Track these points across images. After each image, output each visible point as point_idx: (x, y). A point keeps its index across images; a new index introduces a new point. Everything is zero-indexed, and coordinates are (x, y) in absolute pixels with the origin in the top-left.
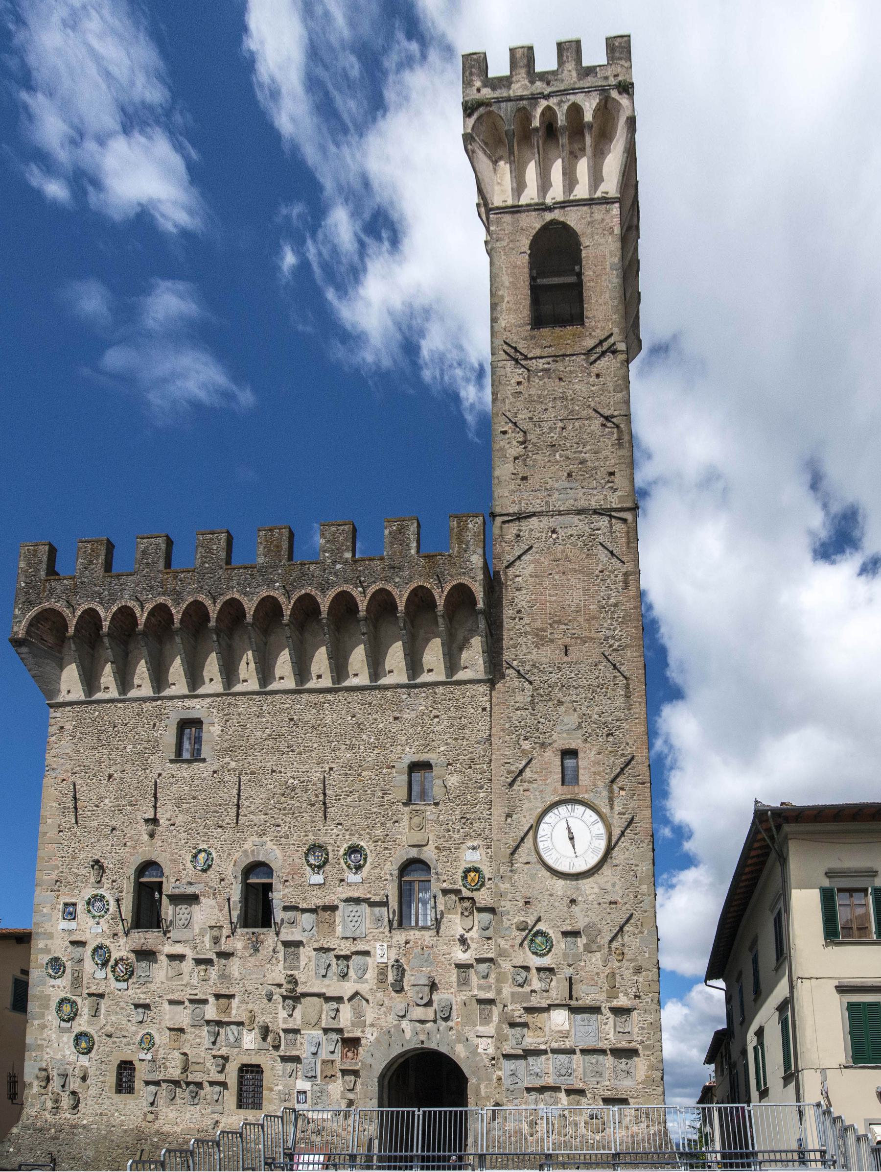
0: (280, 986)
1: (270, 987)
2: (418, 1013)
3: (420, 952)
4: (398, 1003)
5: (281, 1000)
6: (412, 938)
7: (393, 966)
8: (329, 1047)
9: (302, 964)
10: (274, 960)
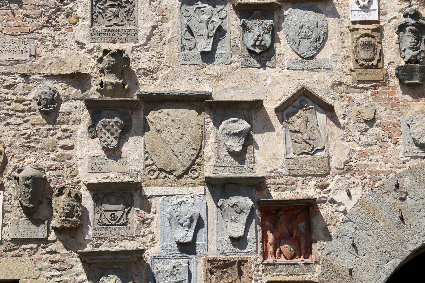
0: (79, 79)
1: (49, 83)
5: (85, 115)
8: (226, 226)
9: (144, 26)
10: (61, 18)
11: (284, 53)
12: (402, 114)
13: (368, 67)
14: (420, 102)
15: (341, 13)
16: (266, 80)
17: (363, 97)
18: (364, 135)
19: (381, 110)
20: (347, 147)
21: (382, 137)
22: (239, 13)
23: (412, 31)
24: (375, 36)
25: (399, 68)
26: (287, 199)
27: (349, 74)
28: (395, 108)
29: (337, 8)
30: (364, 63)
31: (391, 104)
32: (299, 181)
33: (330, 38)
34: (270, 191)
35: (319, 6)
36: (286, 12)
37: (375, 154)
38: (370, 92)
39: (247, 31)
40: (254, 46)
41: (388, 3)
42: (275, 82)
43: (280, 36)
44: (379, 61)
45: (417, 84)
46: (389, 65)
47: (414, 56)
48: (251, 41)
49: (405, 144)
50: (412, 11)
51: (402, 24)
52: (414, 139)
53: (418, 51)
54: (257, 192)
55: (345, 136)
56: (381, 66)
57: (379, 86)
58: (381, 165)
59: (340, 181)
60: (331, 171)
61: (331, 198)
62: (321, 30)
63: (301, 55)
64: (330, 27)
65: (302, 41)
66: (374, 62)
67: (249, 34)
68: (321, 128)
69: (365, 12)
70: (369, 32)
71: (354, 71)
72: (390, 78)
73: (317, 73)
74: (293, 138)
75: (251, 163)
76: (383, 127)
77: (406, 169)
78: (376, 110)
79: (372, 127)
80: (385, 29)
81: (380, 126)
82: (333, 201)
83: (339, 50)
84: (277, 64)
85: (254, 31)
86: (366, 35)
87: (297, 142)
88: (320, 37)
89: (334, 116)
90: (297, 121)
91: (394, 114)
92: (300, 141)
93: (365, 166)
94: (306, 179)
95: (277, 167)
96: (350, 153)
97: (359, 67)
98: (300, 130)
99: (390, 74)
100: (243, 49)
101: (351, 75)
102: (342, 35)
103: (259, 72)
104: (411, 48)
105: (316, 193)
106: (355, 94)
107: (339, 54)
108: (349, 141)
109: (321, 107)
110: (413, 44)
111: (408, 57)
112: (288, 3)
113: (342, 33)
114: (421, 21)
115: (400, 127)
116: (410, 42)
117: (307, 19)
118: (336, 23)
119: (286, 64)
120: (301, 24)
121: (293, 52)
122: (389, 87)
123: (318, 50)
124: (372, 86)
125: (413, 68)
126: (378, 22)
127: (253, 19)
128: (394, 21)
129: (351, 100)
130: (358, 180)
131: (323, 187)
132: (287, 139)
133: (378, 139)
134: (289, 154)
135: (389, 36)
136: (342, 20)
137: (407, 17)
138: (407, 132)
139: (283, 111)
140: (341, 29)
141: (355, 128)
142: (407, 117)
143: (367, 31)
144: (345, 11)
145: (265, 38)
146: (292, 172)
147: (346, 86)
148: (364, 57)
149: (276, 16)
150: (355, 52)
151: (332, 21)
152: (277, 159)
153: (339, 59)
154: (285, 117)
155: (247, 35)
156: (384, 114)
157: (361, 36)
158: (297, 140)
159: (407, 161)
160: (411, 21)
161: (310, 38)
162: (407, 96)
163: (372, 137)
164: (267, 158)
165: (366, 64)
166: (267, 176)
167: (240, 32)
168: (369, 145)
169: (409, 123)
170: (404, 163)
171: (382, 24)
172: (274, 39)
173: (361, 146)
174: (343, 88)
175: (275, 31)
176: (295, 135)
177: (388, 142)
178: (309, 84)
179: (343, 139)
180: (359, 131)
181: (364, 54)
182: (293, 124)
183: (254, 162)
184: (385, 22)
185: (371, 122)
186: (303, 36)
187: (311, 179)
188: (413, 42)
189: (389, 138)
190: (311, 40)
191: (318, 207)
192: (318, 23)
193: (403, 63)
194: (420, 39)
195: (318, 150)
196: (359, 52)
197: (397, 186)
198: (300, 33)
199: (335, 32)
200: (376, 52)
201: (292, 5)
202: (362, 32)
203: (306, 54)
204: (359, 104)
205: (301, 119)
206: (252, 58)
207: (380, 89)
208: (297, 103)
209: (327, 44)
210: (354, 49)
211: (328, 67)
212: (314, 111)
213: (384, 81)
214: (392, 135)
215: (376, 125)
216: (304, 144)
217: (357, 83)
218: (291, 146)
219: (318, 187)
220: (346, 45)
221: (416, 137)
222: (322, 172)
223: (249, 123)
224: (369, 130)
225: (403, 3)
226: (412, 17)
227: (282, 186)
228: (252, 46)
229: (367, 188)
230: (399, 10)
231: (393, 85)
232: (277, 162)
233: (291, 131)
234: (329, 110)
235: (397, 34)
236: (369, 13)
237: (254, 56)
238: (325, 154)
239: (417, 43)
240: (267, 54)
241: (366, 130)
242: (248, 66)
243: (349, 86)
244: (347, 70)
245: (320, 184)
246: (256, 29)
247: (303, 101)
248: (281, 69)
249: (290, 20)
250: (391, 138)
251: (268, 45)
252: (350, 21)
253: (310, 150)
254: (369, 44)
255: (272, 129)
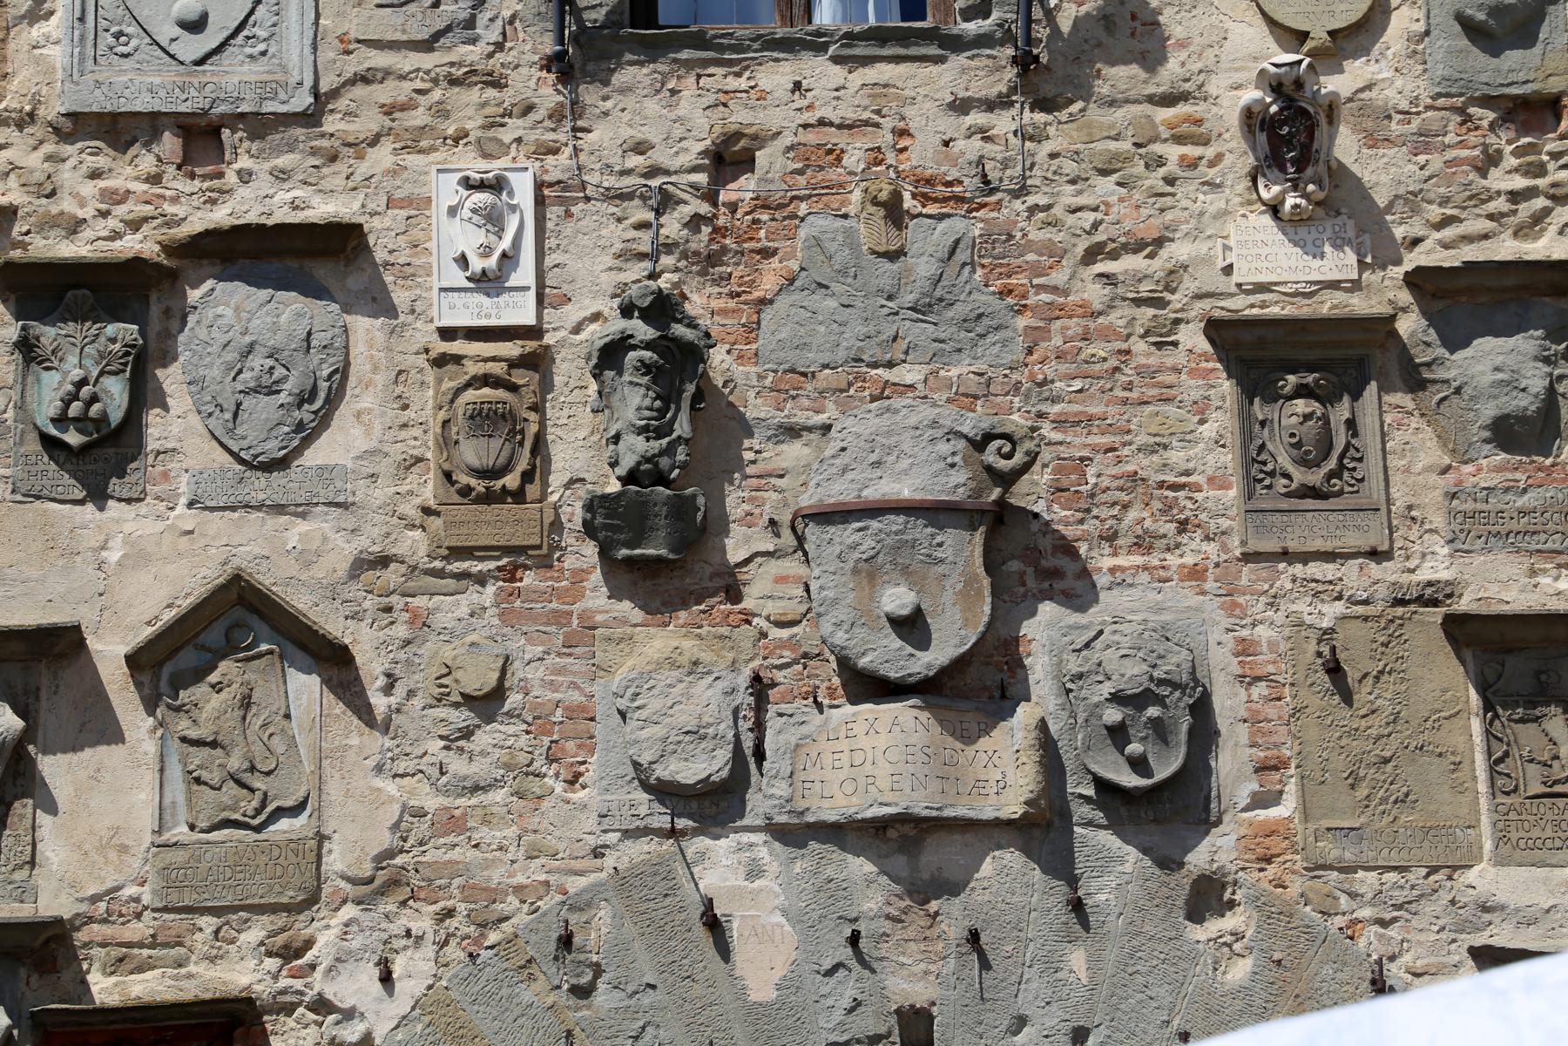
2: (870, 758)
3: (871, 231)
4: (665, 683)
6: (779, 117)
7: (610, 356)
11: (178, 445)
12: (602, 673)
13: (488, 498)
14: (671, 627)
15: (400, 297)
16: (103, 548)
17: (463, 611)
18: (461, 749)
19: (527, 657)
20: (392, 799)
21: (523, 758)
22: (13, 297)
23: (645, 367)
24: (521, 382)
25: (594, 504)
26: (147, 999)
27: (417, 523)
28: (577, 651)
29: (388, 279)
30: (473, 482)
31: (566, 635)
32: (201, 930)
33: (357, 391)
34: (88, 971)
35: (322, 272)
36: (194, 295)
37: (495, 821)
38: (490, 589)
39: (39, 363)
40: (61, 420)
41: (575, 265)
42: (138, 557)
43: (168, 381)
44: (527, 477)
45: (659, 560)
46: (568, 492)
47: (648, 460)
48: (51, 402)
49: (604, 783)
50: (645, 295)
51: (612, 341)
52: (636, 765)
53: (667, 440)
54: (34, 979)
55: (390, 755)
56: (537, 495)
57: (526, 567)
58: (513, 862)
59: (355, 928)
60: (326, 890)
61: (316, 990)
62: (322, 361)
63: (243, 454)
64: (358, 350)
65: (248, 402)
66: (511, 481)
67: (45, 375)
68: (299, 726)
69: (488, 295)
70: (498, 369)
71: (438, 514)
72: (568, 539)
73: (299, 520)
74: (191, 767)
75: (19, 867)
76: (530, 719)
77: (604, 875)
78: (507, 658)
79: (490, 720)
80: (558, 358)
81: (519, 716)
82: (322, 1006)
83: (383, 437)
84: (148, 487)
85: (66, 366)
86: (485, 380)
87: (206, 784)
88: (315, 386)
89: (349, 683)
90: (209, 704)
91: (574, 673)
92: (214, 777)
93: (454, 869)
94: (227, 923)
95: (121, 879)
96: (400, 820)
97: (457, 498)
98: (220, 738)
99: (569, 525)
100: (23, 432)
101: (424, 530)
102: (402, 378)
103: (78, 519)
104: (642, 430)
105: (259, 976)
106: (436, 598)
107: (386, 449)
108: (402, 776)
109: (303, 647)
110: (647, 413)
111: (628, 462)
112: (205, 262)
113: (400, 372)
114: (679, 330)
115: (592, 719)
116: (639, 409)
117: (269, 319)
118: (380, 337)
119: (183, 488)
120: (248, 339)
121: (214, 443)
122: (561, 570)
123: (308, 434)
124: (499, 569)
125: (644, 503)
126: (534, 332)
127: (65, 321)
128: (593, 327)
129: (421, 622)
130: (421, 921)
131: (290, 953)
132: (167, 773)
133: (508, 767)
134: (170, 829)
135: (573, 384)
136: (404, 325)
137: (631, 318)
138: (614, 737)
139: (160, 664)
140: (399, 358)
141: (426, 725)
142: (616, 682)
143: (490, 364)
144: (418, 292)
145: (106, 392)
146: (174, 899)
147: (403, 569)
148: (476, 463)
149: (155, 310)
150: (446, 442)
151: (364, 327)
152: (123, 849)
153: (385, 467)
154: (164, 686)
155: (38, 381)
156: (535, 674)
157: (468, 385)
158: (205, 775)
159: (607, 846)
160: (642, 330)
161: (278, 392)
162: (626, 605)
163: (489, 760)
164: (87, 847)
165: (479, 486)
166: (78, 915)
167: (13, 367)
168: (476, 789)
169: (622, 703)
170: (597, 853)
171: (549, 339)
172: (143, 394)
173: (447, 793)
174: (392, 576)
175: (150, 366)
176: (198, 756)
177: (545, 775)
178: (265, 563)
179: (379, 769)
180: (441, 737)
181: (473, 452)
182: (195, 713)
183: (32, 863)
184: (562, 334)
185: (488, 703)
186: (252, 385)
187: (246, 921)
188: (648, 409)
189: (551, 760)
190: (283, 398)
191: (265, 1030)
192: (309, 334)
193: (614, 487)
194: (674, 395)
195: (280, 812)
196: (457, 442)
197: (566, 941)
198: (240, 372)
199: (375, 369)
200: (521, 443)
201: (217, 269)
202: (473, 369)
203: (259, 450)
204: (451, 635)
205: (223, 695)
206: (53, 466)
207: (529, 579)
208: (214, 636)
209: (344, 412)
210: (439, 430)
211: (341, 499)
212: (278, 665)
213: (545, 550)
214: (563, 750)
215: (507, 714)
216: (231, 789)
217: (444, 558)
218: (181, 798)
219: (269, 954)
220: (413, 415)
221: (644, 759)
222: (291, 893)
223: (20, 712)
224: (478, 733)
225: (629, 265)
226: (646, 315)
227: (136, 951)
228: (52, 420)
229: (454, 952)
230: (610, 291)
231: (578, 565)
232: (122, 862)
233: (184, 739)
234: (333, 662)
235: (594, 376)
236: (505, 297)
237: (61, 460)
238: (308, 825)
239: (662, 412)
240: (111, 451)
241: (467, 734)
242: (38, 497)
243: (415, 568)
244: (410, 509)
245: (280, 940)
246: (73, 359)
247: (237, 625)
248: (162, 506)
249: (205, 322)
250: (556, 760)
251: (116, 416)
252: (432, 327)
253: (250, 813)
254: (495, 412)
255: (111, 733)
